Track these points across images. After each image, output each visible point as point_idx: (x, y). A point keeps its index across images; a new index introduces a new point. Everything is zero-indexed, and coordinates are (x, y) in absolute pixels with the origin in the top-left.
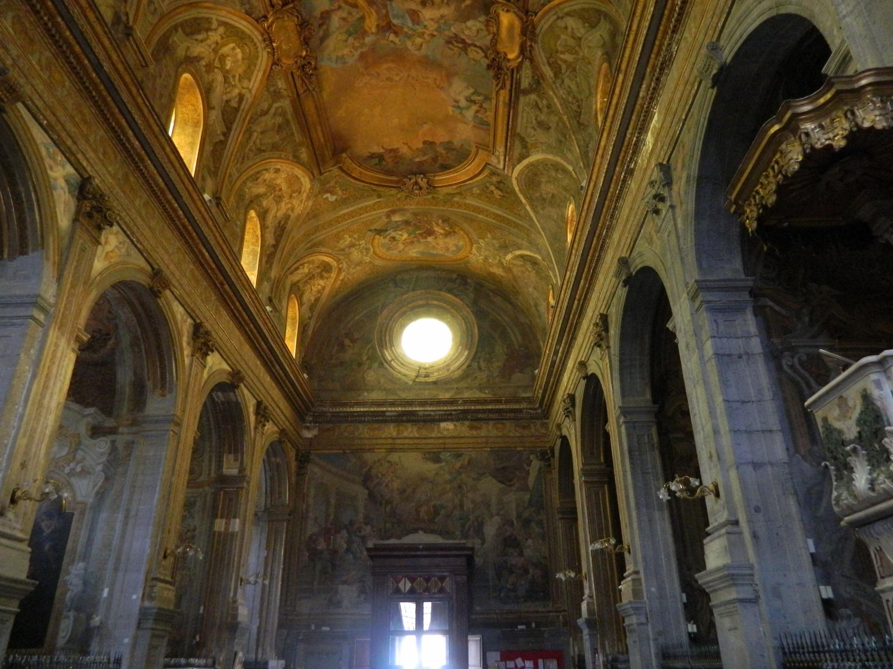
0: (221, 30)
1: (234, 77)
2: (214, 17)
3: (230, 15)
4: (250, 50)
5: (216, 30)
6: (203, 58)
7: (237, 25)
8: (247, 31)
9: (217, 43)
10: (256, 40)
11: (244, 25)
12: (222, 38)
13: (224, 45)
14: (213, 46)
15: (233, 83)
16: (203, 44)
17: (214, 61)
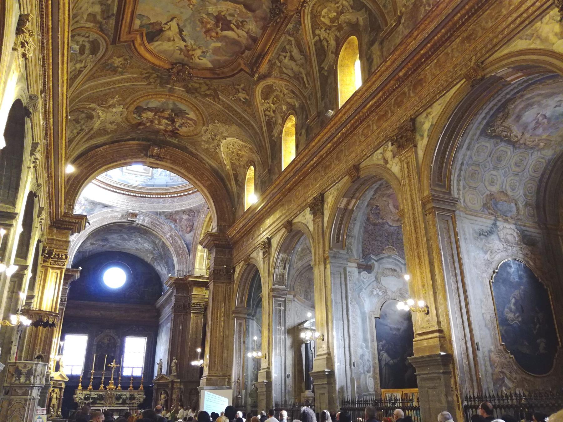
0: (317, 32)
1: (338, 7)
2: (313, 41)
3: (308, 33)
4: (318, 7)
5: (319, 35)
6: (336, 36)
7: (310, 25)
8: (309, 16)
9: (326, 30)
10: (310, 9)
11: (307, 21)
12: (322, 28)
13: (325, 25)
14: (328, 31)
15: (341, 7)
16: (329, 39)
17: (335, 26)
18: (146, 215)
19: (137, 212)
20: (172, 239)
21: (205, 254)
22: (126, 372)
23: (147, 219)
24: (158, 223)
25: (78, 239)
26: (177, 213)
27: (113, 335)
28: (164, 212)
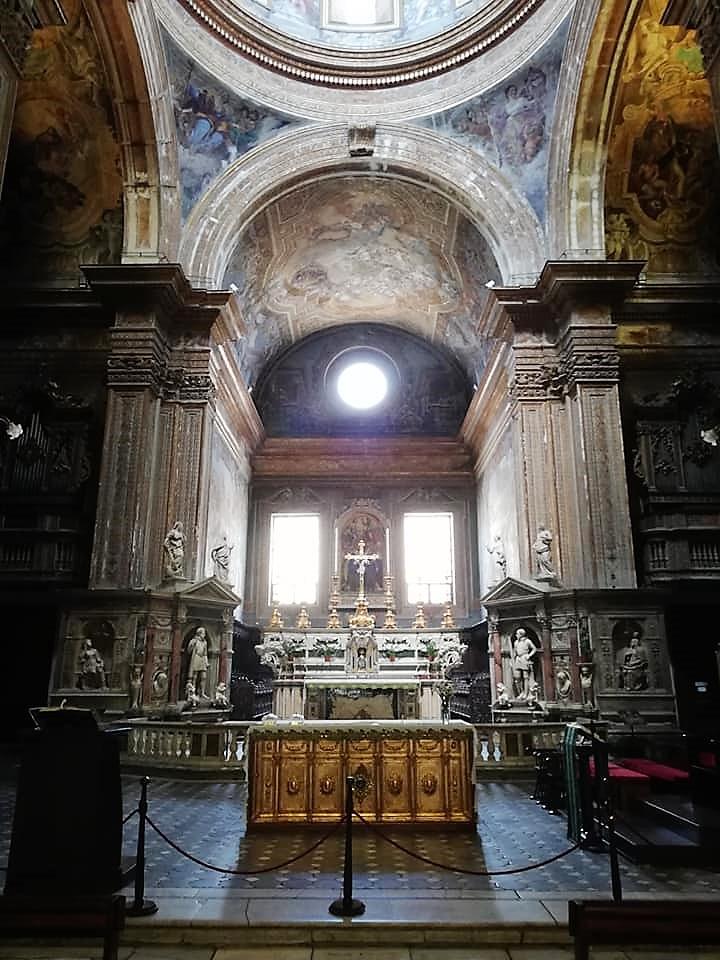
18: (400, 131)
19: (372, 123)
20: (483, 191)
21: (596, 205)
22: (415, 595)
23: (403, 144)
24: (436, 151)
25: (222, 219)
26: (487, 100)
27: (375, 512)
28: (448, 113)
